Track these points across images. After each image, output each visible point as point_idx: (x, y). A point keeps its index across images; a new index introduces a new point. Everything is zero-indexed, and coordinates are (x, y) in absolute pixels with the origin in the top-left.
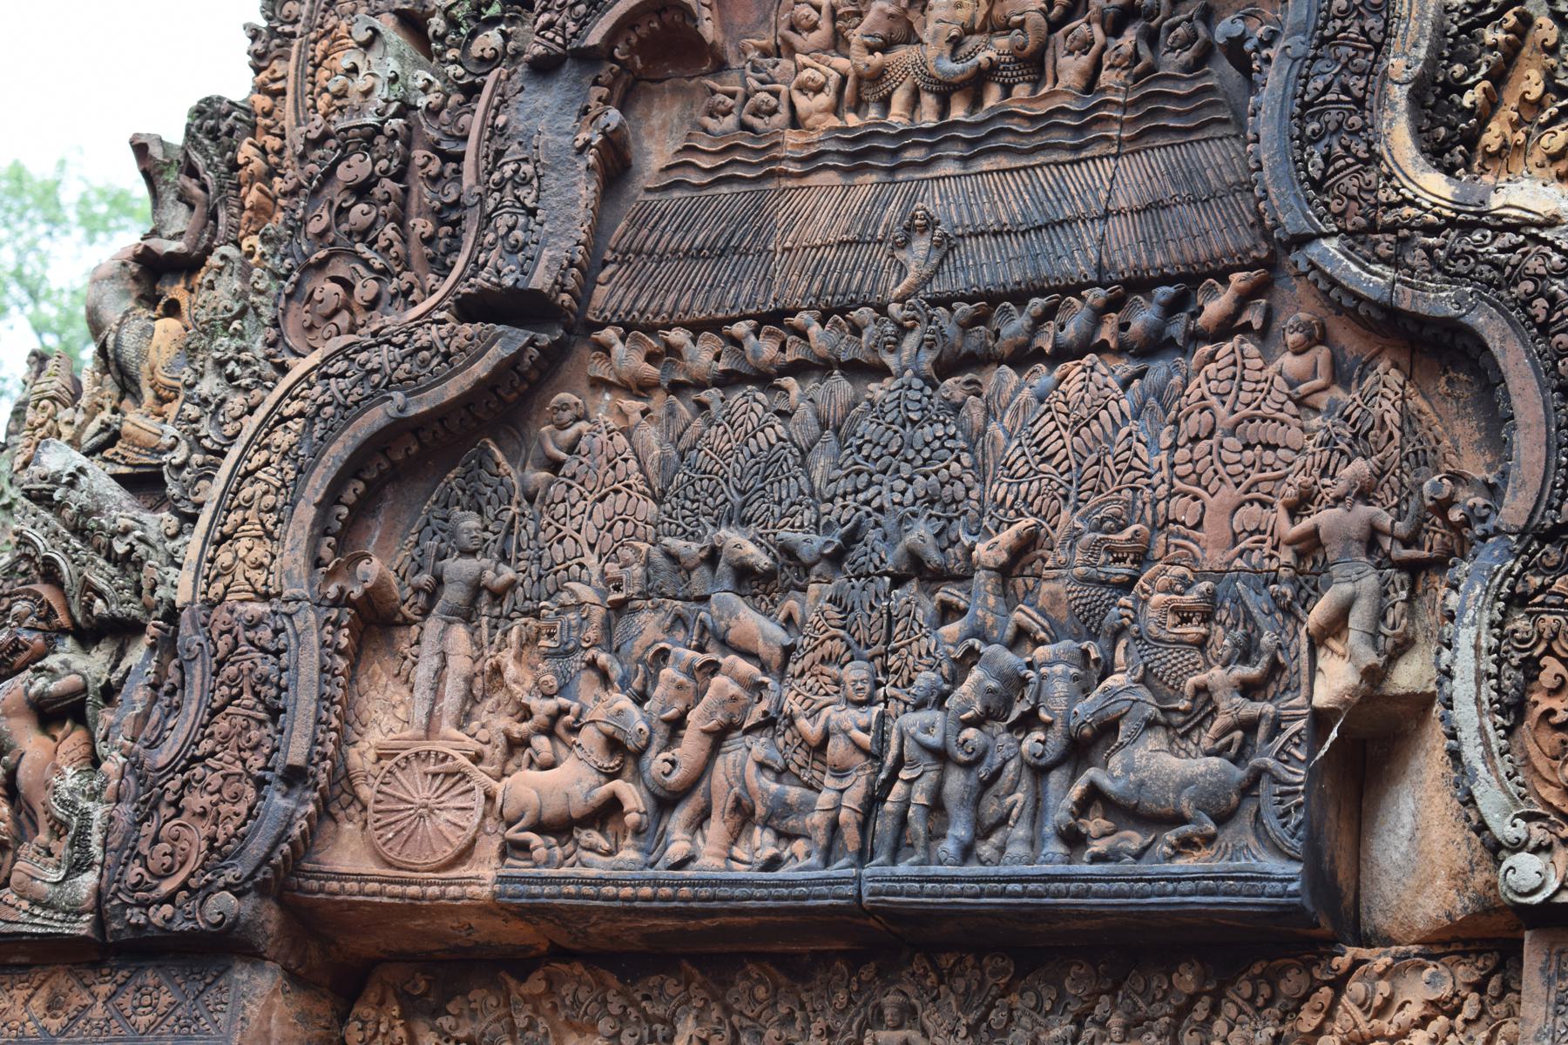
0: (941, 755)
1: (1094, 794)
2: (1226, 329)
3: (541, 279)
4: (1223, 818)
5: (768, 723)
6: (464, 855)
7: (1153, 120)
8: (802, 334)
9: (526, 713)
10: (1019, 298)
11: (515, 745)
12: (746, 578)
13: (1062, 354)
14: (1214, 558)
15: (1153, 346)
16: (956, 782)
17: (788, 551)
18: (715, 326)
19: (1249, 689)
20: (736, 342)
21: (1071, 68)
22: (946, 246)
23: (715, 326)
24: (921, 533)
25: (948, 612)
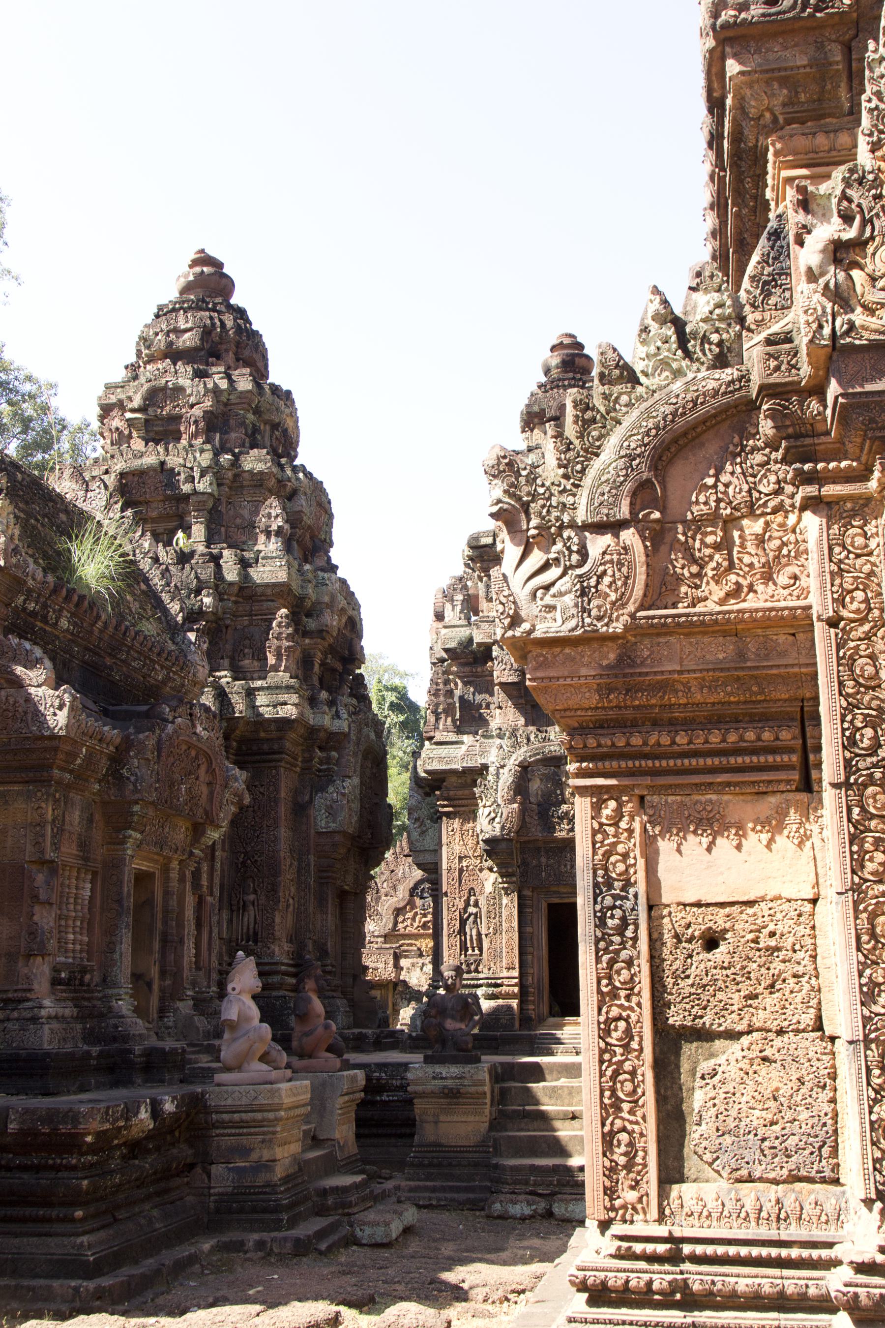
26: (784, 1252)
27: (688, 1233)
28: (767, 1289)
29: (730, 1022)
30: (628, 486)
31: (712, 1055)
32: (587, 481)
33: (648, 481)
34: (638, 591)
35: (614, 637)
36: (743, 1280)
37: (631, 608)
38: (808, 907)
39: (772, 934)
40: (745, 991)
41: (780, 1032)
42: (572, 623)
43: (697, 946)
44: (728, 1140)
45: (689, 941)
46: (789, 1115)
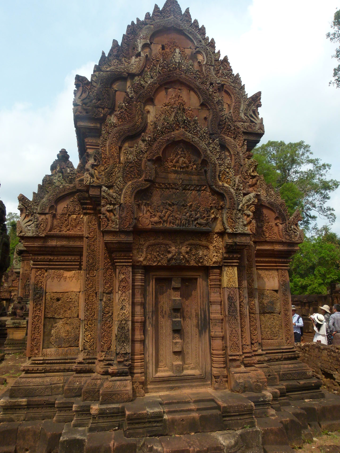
0: (186, 220)
1: (197, 223)
2: (204, 190)
3: (152, 179)
4: (206, 225)
5: (172, 216)
6: (148, 225)
7: (198, 174)
8: (172, 186)
9: (152, 214)
10: (188, 185)
11: (151, 216)
12: (170, 205)
13: (192, 190)
14: (204, 207)
15: (198, 191)
16: (187, 221)
17: (173, 203)
18: (164, 184)
19: (207, 216)
20: (166, 186)
21: (191, 168)
22: (183, 181)
23: (164, 184)
24: (183, 203)
25: (185, 209)
26: (66, 361)
27: (47, 358)
28: (62, 368)
29: (61, 316)
30: (49, 206)
31: (56, 323)
32: (40, 204)
33: (53, 205)
34: (48, 228)
35: (42, 237)
36: (57, 367)
37: (47, 232)
38: (78, 293)
39: (71, 299)
40: (64, 309)
41: (70, 318)
42: (34, 234)
43: (55, 301)
44: (57, 340)
45: (54, 300)
46: (70, 334)
